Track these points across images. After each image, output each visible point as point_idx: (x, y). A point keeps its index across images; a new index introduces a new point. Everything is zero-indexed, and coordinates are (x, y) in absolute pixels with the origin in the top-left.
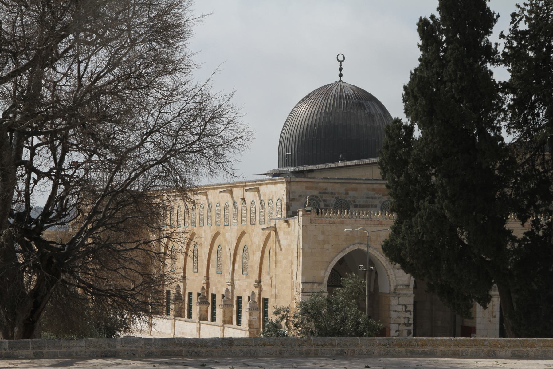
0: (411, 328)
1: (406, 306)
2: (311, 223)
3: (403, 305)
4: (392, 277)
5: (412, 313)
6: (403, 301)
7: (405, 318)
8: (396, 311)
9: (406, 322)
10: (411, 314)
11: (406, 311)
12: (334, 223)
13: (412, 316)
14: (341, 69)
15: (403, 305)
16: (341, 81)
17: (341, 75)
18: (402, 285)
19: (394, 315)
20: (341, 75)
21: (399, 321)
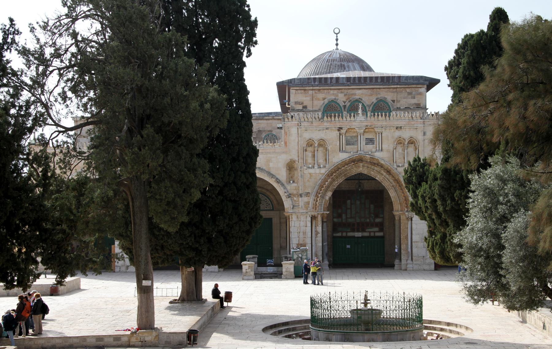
14: (337, 40)
16: (337, 49)
17: (337, 45)
20: (337, 45)
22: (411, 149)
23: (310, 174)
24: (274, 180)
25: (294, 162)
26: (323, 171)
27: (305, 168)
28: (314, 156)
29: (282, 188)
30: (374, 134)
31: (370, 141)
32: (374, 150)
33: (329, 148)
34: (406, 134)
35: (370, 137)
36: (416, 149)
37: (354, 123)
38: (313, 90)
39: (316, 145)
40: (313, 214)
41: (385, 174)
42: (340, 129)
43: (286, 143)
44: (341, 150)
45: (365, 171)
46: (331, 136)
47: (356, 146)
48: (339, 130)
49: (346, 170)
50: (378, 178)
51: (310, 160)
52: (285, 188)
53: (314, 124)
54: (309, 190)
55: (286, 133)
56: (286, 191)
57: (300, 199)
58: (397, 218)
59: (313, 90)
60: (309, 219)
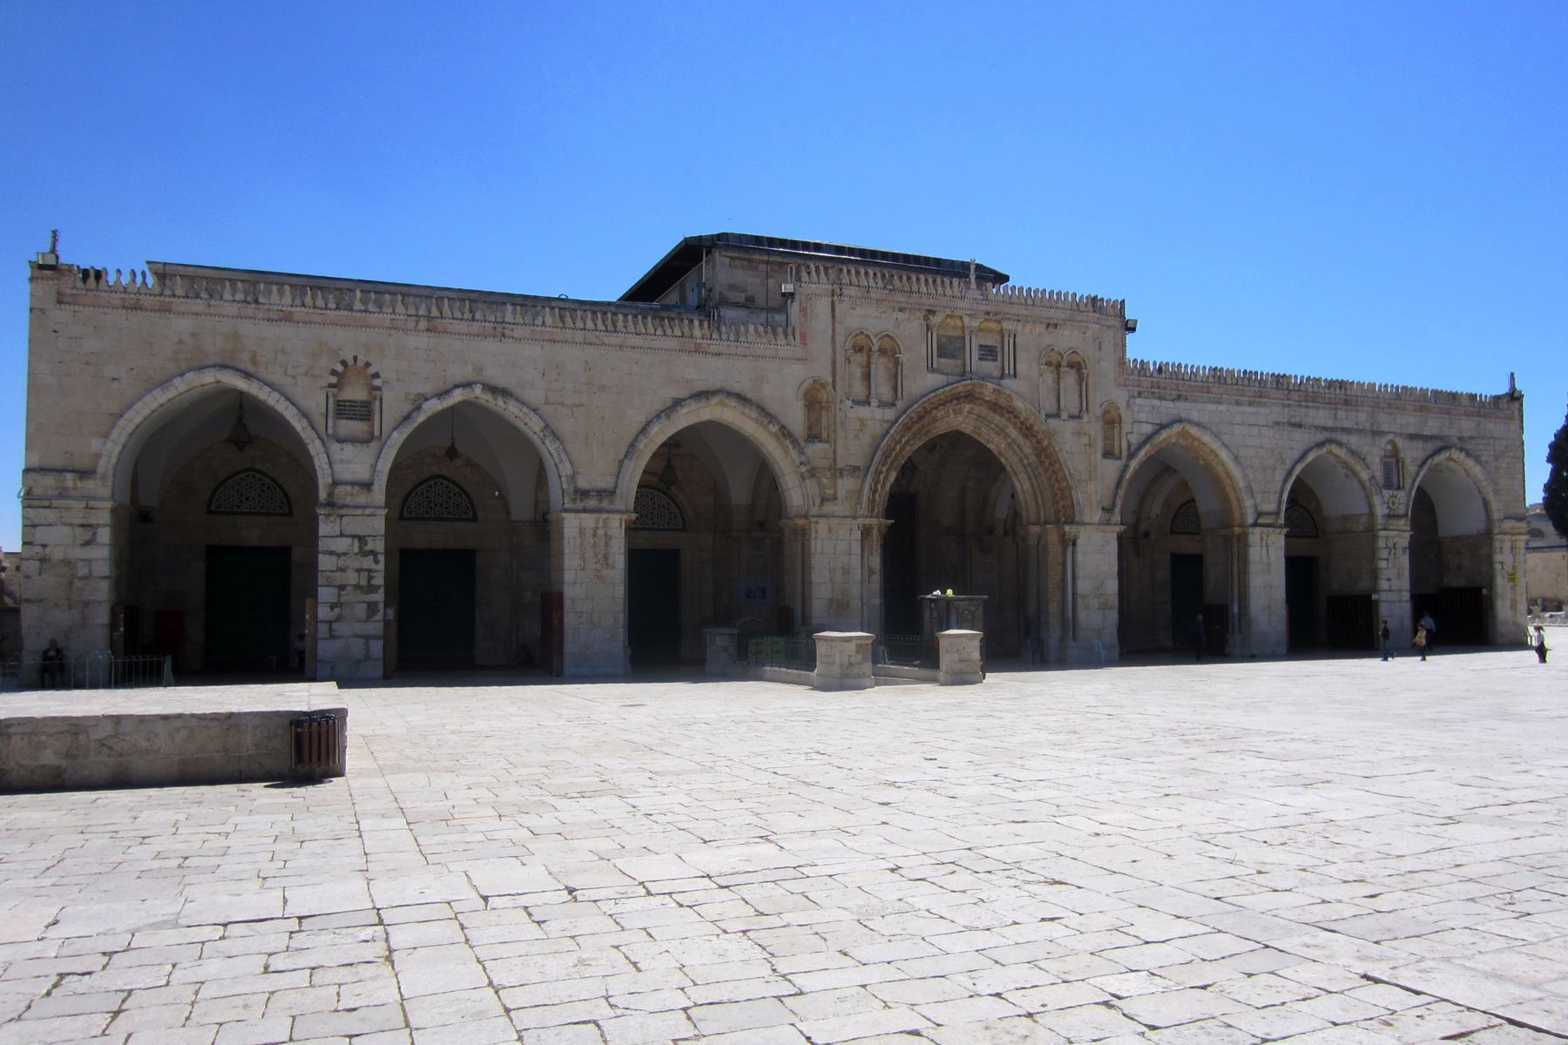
0: (379, 596)
1: (362, 539)
2: (60, 302)
3: (353, 537)
4: (320, 462)
5: (381, 558)
6: (355, 525)
7: (359, 571)
8: (332, 553)
9: (363, 583)
10: (376, 562)
11: (363, 553)
12: (136, 307)
13: (381, 566)
15: (353, 537)
18: (353, 484)
19: (325, 563)
21: (339, 578)
22: (1069, 380)
23: (861, 420)
24: (774, 428)
25: (823, 386)
26: (890, 414)
27: (850, 403)
28: (867, 377)
29: (794, 453)
30: (998, 337)
31: (988, 352)
32: (997, 373)
33: (903, 357)
34: (1067, 340)
35: (989, 343)
36: (1081, 379)
37: (961, 304)
38: (767, 262)
39: (875, 348)
40: (868, 521)
41: (1014, 433)
42: (932, 312)
43: (803, 336)
44: (932, 369)
45: (967, 429)
46: (909, 330)
47: (959, 362)
48: (926, 318)
49: (935, 420)
50: (995, 444)
51: (858, 389)
52: (802, 452)
53: (873, 295)
54: (859, 461)
55: (803, 311)
56: (803, 459)
57: (839, 481)
58: (1032, 542)
59: (767, 262)
60: (857, 535)
